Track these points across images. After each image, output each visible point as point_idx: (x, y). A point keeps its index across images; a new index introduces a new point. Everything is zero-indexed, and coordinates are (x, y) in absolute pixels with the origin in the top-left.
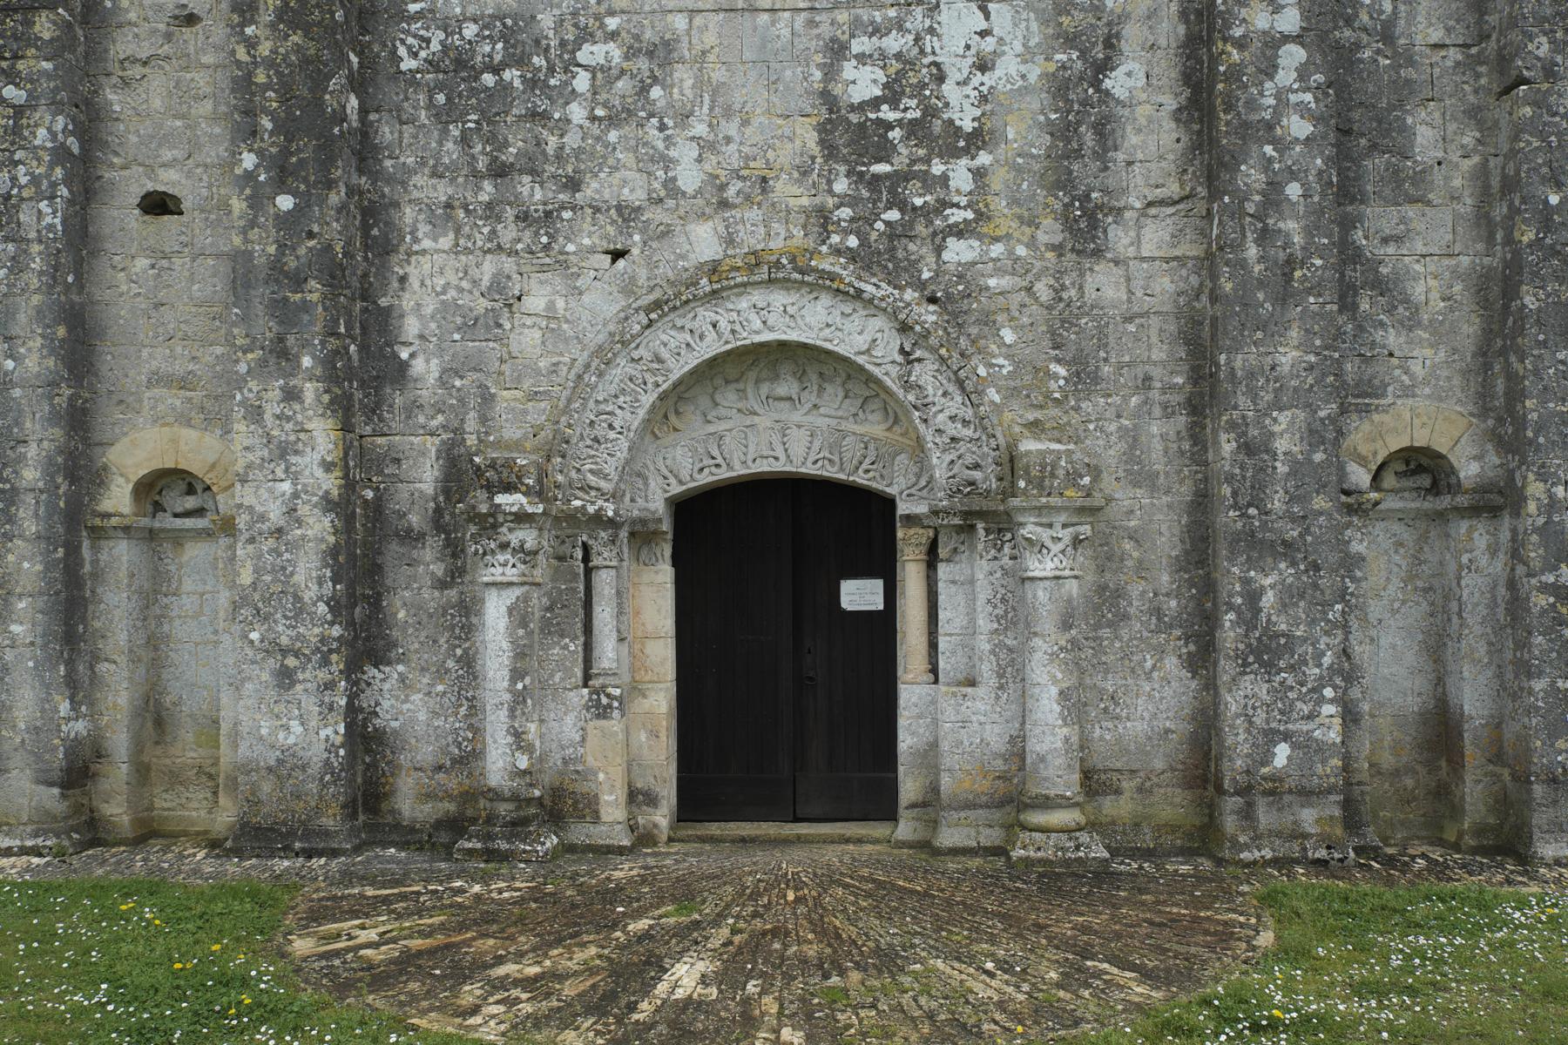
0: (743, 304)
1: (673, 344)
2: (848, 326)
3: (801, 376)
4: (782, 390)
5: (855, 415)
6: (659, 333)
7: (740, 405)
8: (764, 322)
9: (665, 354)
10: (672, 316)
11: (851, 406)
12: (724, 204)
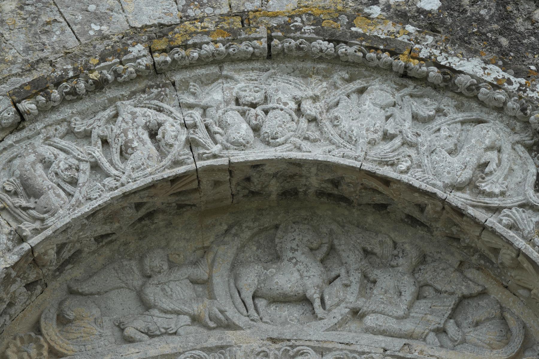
0: (216, 95)
1: (62, 162)
2: (426, 138)
3: (328, 255)
4: (286, 278)
5: (441, 331)
6: (38, 141)
7: (197, 308)
8: (256, 129)
9: (41, 178)
10: (66, 111)
11: (430, 313)
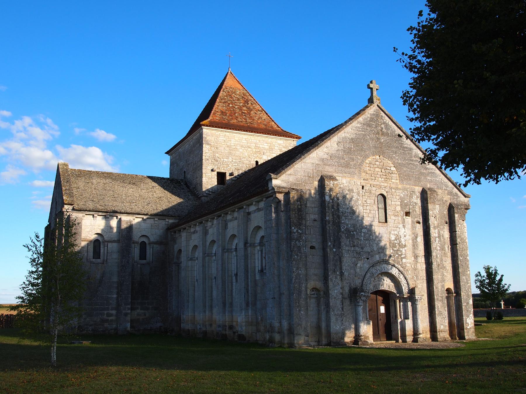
12: (379, 252)
